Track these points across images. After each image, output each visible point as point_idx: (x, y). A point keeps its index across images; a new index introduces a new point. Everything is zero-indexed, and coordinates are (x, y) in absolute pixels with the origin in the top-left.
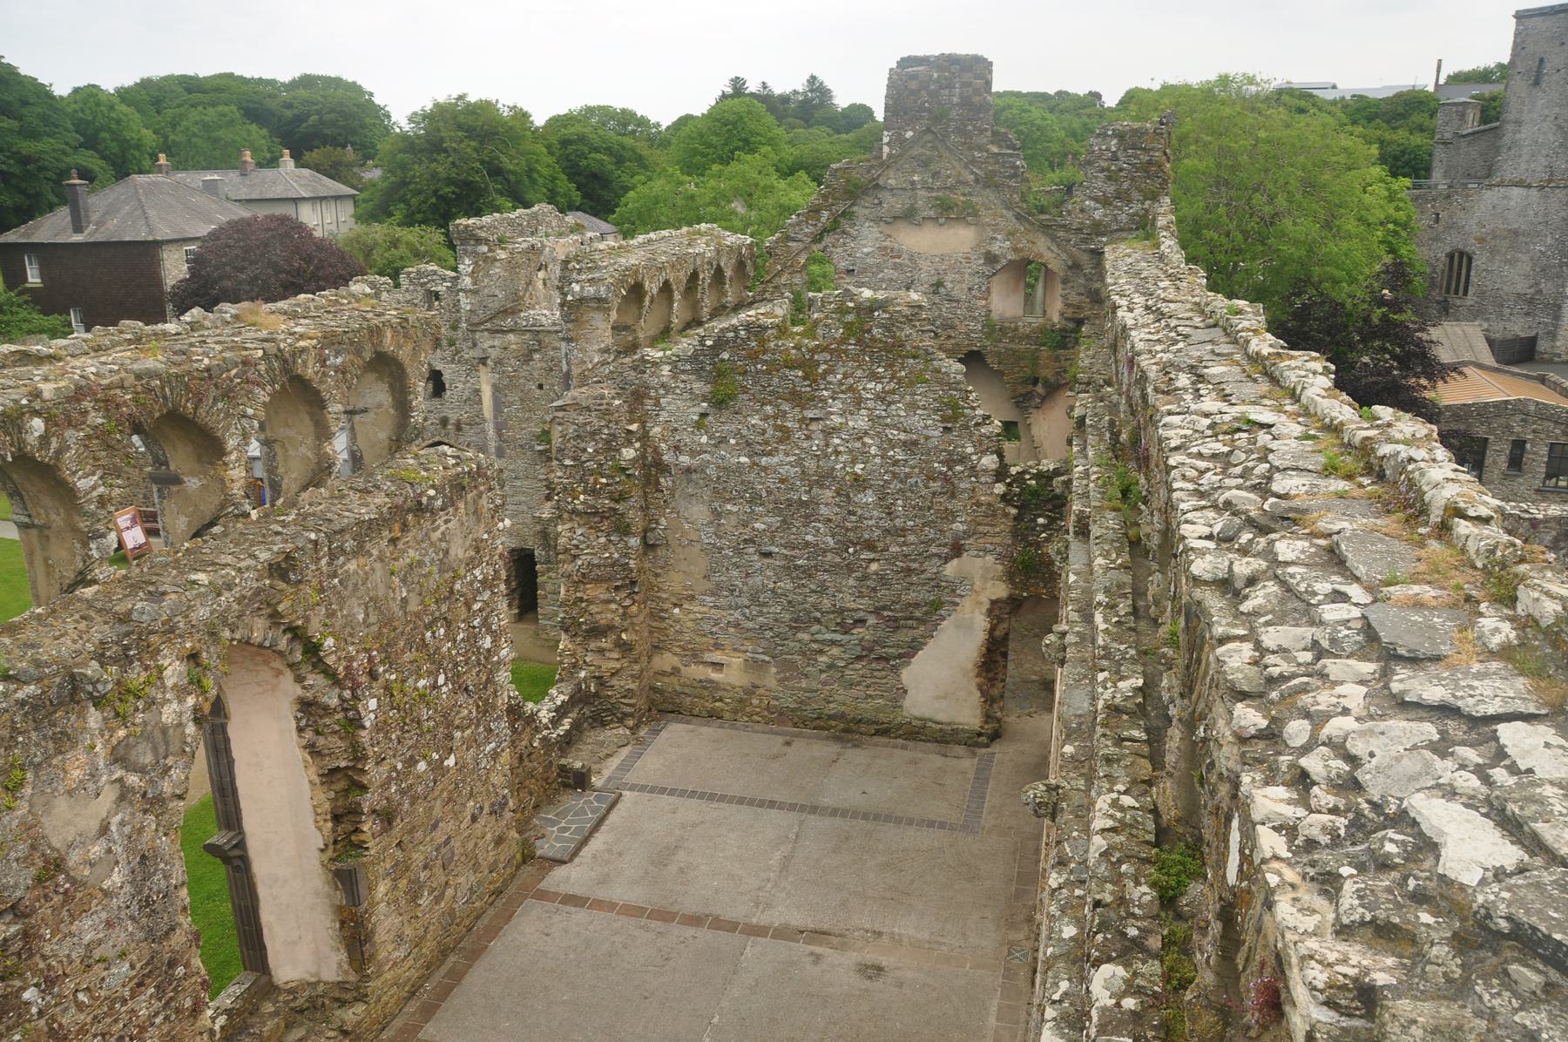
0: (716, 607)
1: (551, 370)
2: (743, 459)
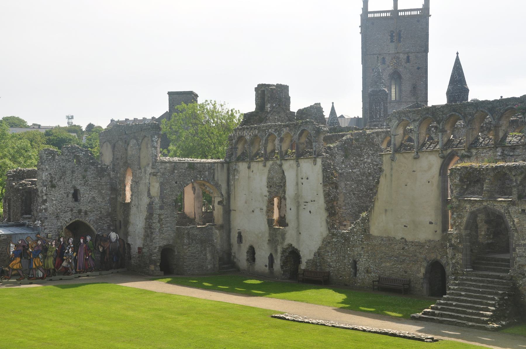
0: (345, 209)
1: (180, 176)
2: (350, 170)
